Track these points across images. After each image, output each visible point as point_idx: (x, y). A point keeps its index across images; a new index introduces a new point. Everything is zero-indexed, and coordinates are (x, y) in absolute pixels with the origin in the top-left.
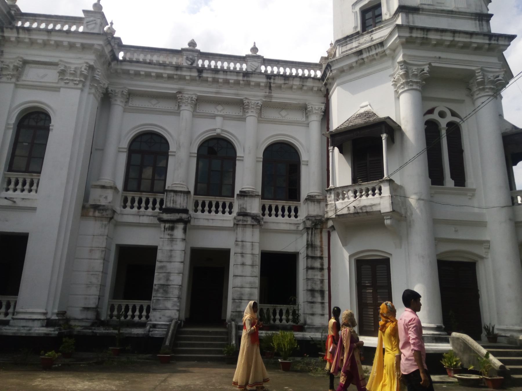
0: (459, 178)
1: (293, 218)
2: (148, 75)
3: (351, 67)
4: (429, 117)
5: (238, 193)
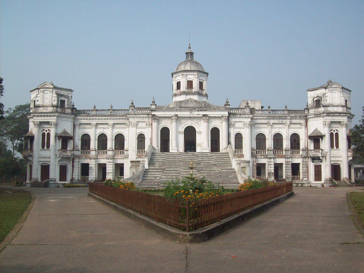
0: (337, 147)
1: (298, 154)
2: (260, 119)
3: (313, 117)
4: (331, 132)
5: (285, 149)
